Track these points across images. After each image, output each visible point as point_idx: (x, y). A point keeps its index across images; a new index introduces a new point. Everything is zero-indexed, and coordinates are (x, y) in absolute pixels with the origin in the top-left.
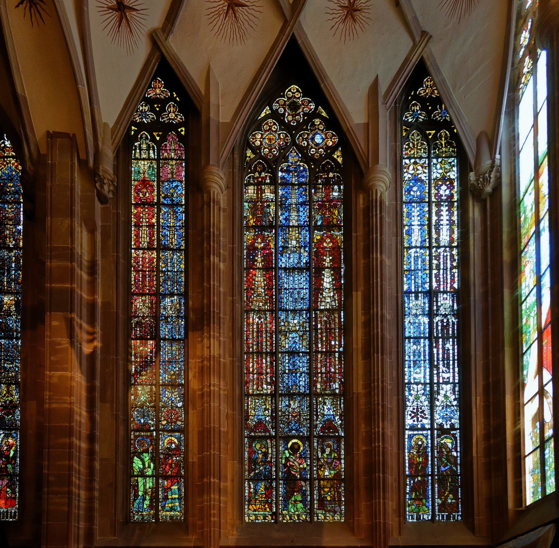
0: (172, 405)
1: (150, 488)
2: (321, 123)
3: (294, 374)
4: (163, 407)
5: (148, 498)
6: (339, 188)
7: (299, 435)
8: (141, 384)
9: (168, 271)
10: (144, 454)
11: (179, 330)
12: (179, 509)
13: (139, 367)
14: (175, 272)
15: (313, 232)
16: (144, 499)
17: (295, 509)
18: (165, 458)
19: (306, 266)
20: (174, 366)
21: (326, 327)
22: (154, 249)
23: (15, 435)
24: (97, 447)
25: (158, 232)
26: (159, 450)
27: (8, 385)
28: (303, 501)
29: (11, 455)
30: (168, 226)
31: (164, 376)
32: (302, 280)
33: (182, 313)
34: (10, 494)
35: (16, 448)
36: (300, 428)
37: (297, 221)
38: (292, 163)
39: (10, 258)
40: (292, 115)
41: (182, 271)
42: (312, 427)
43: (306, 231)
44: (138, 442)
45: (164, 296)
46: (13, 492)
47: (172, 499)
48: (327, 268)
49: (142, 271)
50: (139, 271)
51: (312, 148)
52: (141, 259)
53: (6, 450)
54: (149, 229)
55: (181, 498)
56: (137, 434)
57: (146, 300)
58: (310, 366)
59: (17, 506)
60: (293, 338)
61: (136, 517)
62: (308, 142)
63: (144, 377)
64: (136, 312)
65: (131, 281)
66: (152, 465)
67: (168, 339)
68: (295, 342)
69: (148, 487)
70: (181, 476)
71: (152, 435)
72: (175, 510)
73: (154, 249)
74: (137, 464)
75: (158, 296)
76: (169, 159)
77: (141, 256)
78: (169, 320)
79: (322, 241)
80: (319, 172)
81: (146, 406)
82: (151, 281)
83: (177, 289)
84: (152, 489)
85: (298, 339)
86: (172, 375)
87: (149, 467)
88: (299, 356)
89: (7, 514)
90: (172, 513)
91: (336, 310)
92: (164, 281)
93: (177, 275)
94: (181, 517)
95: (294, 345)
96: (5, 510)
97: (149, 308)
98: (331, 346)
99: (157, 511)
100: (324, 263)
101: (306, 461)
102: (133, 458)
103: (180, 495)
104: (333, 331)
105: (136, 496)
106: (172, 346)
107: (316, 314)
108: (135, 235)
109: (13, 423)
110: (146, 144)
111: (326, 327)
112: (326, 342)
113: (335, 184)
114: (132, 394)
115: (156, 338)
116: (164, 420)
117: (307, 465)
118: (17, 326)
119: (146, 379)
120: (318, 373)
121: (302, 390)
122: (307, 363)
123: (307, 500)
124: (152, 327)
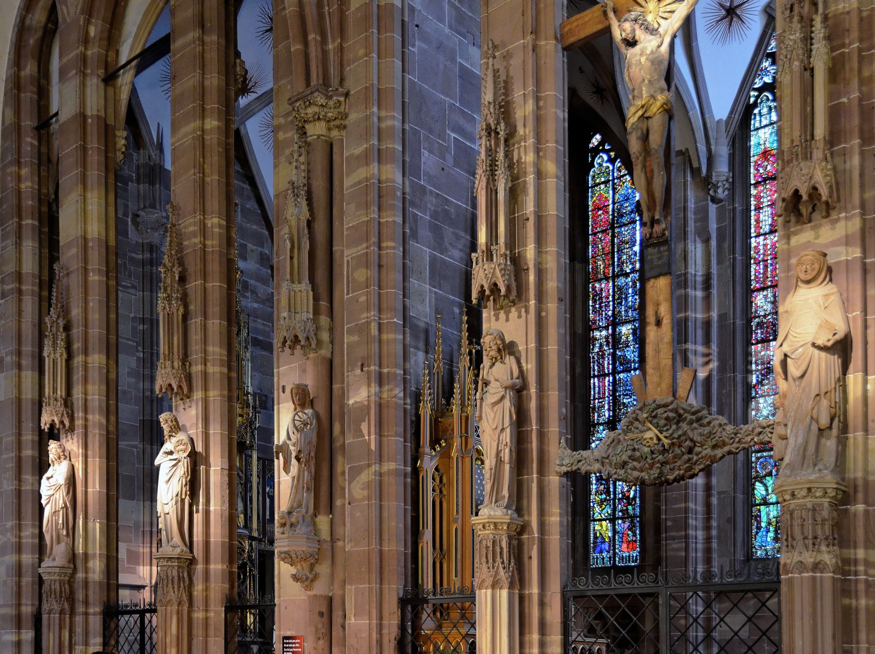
46: (635, 535)
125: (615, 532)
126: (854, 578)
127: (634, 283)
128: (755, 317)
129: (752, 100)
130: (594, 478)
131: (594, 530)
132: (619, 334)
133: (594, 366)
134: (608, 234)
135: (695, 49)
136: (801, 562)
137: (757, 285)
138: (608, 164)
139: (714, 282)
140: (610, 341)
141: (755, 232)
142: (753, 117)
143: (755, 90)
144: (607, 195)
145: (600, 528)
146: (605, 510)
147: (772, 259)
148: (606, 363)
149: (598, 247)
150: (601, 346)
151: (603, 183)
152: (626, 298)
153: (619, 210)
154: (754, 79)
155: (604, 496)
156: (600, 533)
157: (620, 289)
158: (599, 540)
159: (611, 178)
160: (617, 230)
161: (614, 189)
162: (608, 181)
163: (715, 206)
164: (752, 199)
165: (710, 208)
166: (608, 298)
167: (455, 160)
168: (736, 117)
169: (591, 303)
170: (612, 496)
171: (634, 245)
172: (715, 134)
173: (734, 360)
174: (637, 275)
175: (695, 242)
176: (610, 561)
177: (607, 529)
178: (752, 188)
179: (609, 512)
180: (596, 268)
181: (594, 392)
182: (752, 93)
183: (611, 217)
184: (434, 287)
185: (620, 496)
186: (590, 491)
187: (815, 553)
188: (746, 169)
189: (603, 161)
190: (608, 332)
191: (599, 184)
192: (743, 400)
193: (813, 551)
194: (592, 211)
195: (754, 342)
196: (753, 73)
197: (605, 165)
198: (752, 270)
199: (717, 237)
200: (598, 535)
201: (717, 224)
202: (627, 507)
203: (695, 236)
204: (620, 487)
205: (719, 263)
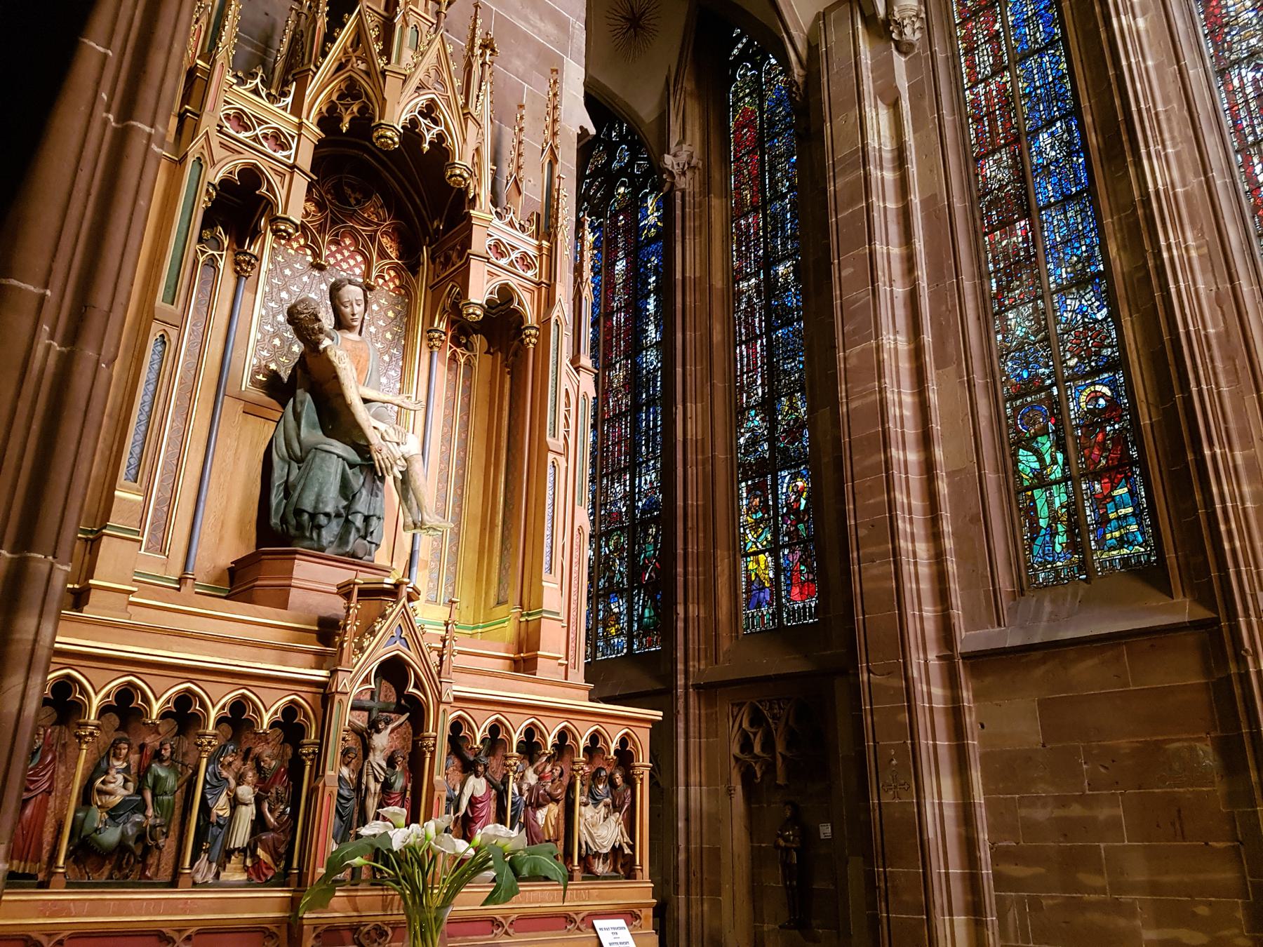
0: (1084, 322)
1: (1062, 506)
5: (1061, 528)
8: (1012, 307)
9: (1036, 88)
10: (1039, 439)
11: (1075, 175)
12: (1140, 539)
13: (1004, 278)
14: (1049, 83)
16: (1054, 534)
27: (790, 396)
29: (802, 508)
30: (1024, 20)
31: (1058, 272)
33: (1075, 145)
34: (806, 576)
39: (784, 208)
41: (1063, 74)
44: (1021, 419)
47: (1119, 518)
52: (983, 98)
53: (795, 501)
55: (1142, 512)
63: (1017, 292)
66: (1060, 457)
69: (1057, 504)
70: (1133, 463)
71: (1050, 395)
72: (1131, 544)
74: (1028, 462)
78: (1052, 168)
81: (1030, 344)
83: (1059, 109)
84: (1068, 506)
86: (1074, 265)
87: (1054, 462)
90: (1125, 551)
93: (1055, 85)
94: (1149, 556)
96: (801, 605)
103: (1136, 505)
105: (1035, 529)
106: (1065, 213)
109: (800, 453)
114: (998, 332)
116: (1072, 357)
118: (798, 300)
119: (1021, 293)
125: (778, 569)
130: (744, 489)
131: (747, 570)
132: (775, 277)
133: (740, 329)
139: (912, 154)
145: (756, 566)
146: (763, 537)
152: (783, 228)
175: (876, 107)
176: (773, 620)
177: (767, 567)
179: (769, 537)
185: (785, 510)
190: (759, 280)
192: (979, 318)
202: (796, 526)
203: (875, 98)
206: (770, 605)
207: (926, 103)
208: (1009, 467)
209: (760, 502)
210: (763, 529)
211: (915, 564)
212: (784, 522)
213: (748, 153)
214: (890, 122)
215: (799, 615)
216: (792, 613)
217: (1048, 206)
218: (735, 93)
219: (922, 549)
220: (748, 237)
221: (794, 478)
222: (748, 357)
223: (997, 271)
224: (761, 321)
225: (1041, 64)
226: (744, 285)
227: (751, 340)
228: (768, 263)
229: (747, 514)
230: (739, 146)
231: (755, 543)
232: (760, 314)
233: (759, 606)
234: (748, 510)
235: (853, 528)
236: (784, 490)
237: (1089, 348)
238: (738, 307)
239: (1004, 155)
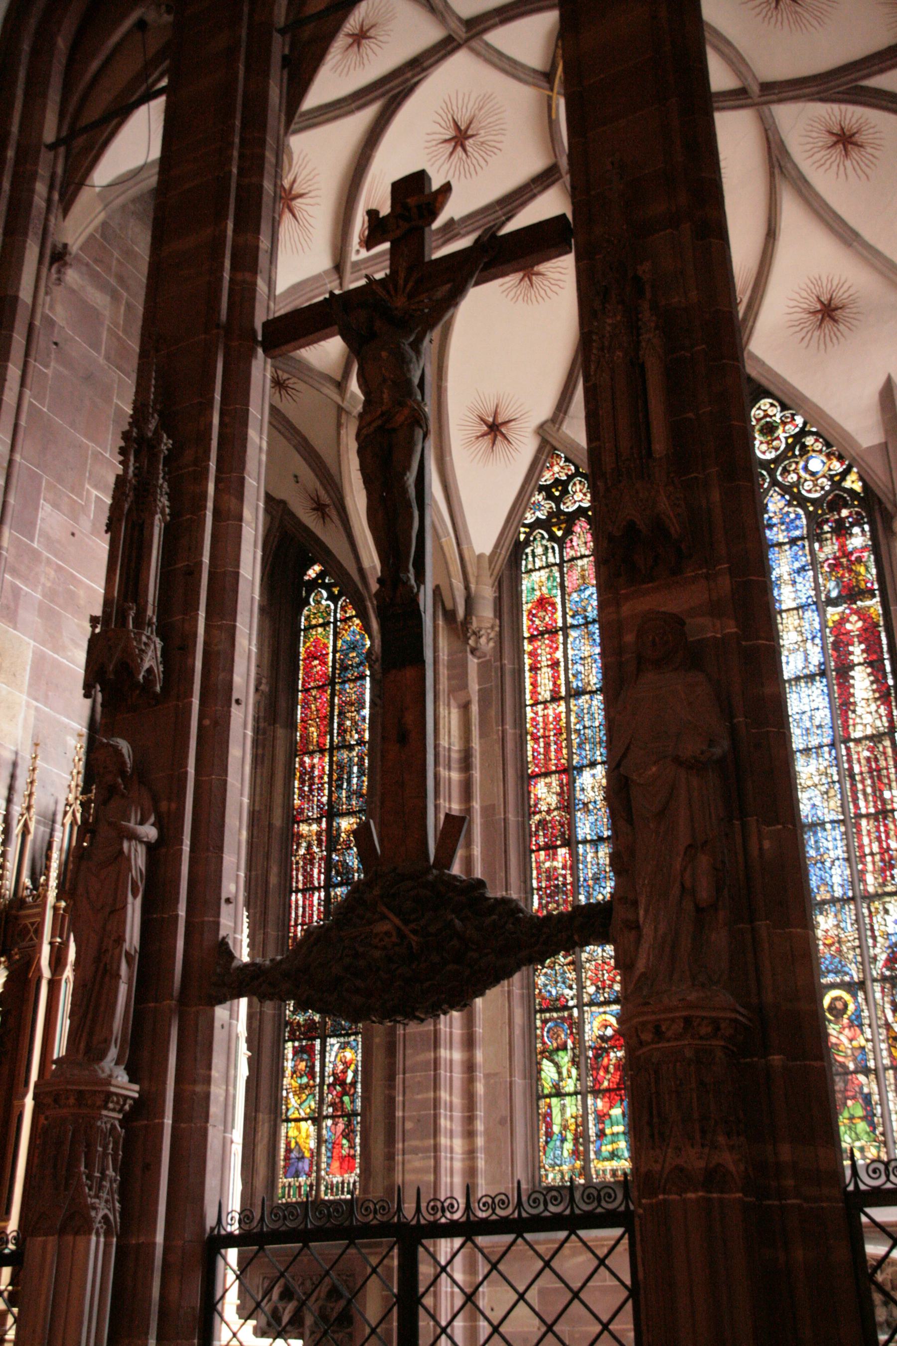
0: (603, 956)
1: (572, 1117)
2: (816, 441)
3: (819, 865)
4: (588, 961)
5: (570, 1136)
6: (863, 531)
7: (842, 981)
15: (825, 611)
16: (563, 1140)
17: (853, 1135)
18: (597, 1056)
19: (820, 669)
20: (603, 884)
21: (870, 767)
22: (561, 698)
23: (354, 1044)
24: (479, 1056)
25: (566, 669)
26: (585, 1041)
28: (869, 1117)
29: (349, 1080)
30: (581, 658)
32: (815, 695)
34: (347, 1150)
35: (357, 1066)
36: (843, 966)
37: (794, 599)
38: (775, 513)
39: (351, 760)
40: (768, 443)
42: (865, 962)
43: (813, 611)
44: (548, 1032)
45: (580, 769)
46: (352, 1147)
47: (613, 1134)
48: (859, 664)
49: (544, 737)
50: (539, 737)
51: (806, 480)
54: (553, 669)
56: (548, 1015)
57: (551, 783)
58: (847, 845)
59: (358, 1171)
60: (810, 799)
61: (551, 1176)
62: (798, 474)
64: (536, 805)
65: (527, 757)
67: (591, 841)
68: (814, 805)
69: (568, 1115)
71: (571, 1016)
72: (619, 1158)
73: (561, 698)
74: (548, 1071)
75: (569, 771)
76: (577, 558)
77: (541, 713)
79: (843, 620)
80: (824, 513)
82: (559, 751)
85: (819, 798)
87: (570, 1077)
88: (825, 830)
89: (343, 1187)
91: (884, 734)
92: (580, 746)
95: (813, 812)
97: (558, 794)
98: (884, 801)
99: (587, 1161)
100: (851, 657)
101: (862, 1033)
102: (539, 1063)
104: (884, 772)
105: (549, 1134)
106: (597, 852)
107: (848, 749)
108: (532, 684)
110: (542, 545)
111: (870, 767)
112: (875, 796)
113: (852, 525)
115: (570, 842)
117: (867, 1040)
120: (865, 855)
121: (838, 893)
122: (842, 840)
123: (875, 1115)
124: (562, 825)
125: (320, 1140)
126: (776, 1203)
127: (361, 759)
128: (535, 813)
129: (522, 537)
131: (287, 1137)
134: (326, 692)
135: (448, 465)
136: (681, 1169)
137: (537, 769)
138: (329, 602)
139: (477, 761)
140: (324, 838)
141: (531, 698)
142: (524, 557)
143: (525, 526)
144: (326, 641)
145: (296, 1133)
146: (306, 1104)
147: (555, 735)
148: (316, 871)
149: (311, 708)
150: (309, 847)
151: (321, 625)
153: (342, 660)
154: (524, 512)
155: (305, 1080)
156: (297, 1143)
157: (341, 767)
158: (294, 1155)
159: (332, 620)
160: (337, 687)
161: (336, 635)
162: (329, 623)
163: (476, 661)
164: (526, 656)
165: (470, 664)
166: (322, 778)
167: (94, 525)
168: (503, 552)
169: (296, 784)
170: (318, 1080)
171: (363, 708)
172: (475, 570)
173: (506, 872)
174: (365, 749)
175: (449, 705)
177: (308, 1136)
178: (526, 642)
179: (313, 1105)
180: (306, 737)
181: (296, 914)
182: (522, 530)
183: (330, 669)
184: (36, 700)
186: (283, 1071)
187: (706, 1150)
188: (518, 619)
189: (322, 598)
191: (316, 626)
193: (703, 1145)
194: (304, 660)
195: (534, 848)
196: (523, 505)
197: (324, 602)
198: (529, 748)
199: (479, 701)
200: (293, 1145)
201: (479, 685)
204: (331, 1066)
205: (482, 736)
206: (309, 1175)
207: (493, 713)
208: (535, 1073)
209: (306, 1067)
210: (307, 1096)
211: (452, 1159)
212: (330, 1092)
213: (318, 688)
214: (459, 722)
215: (337, 1188)
216: (330, 1187)
217: (585, 842)
218: (308, 618)
219: (458, 1144)
220: (312, 778)
221: (343, 1047)
222: (304, 908)
223: (539, 889)
224: (320, 872)
225: (590, 706)
226: (304, 828)
227: (308, 890)
228: (331, 813)
229: (292, 1077)
230: (309, 677)
231: (298, 1110)
232: (320, 865)
233: (297, 1175)
234: (294, 1072)
235: (401, 1120)
236: (332, 1059)
237: (604, 980)
238: (297, 850)
239: (554, 780)
